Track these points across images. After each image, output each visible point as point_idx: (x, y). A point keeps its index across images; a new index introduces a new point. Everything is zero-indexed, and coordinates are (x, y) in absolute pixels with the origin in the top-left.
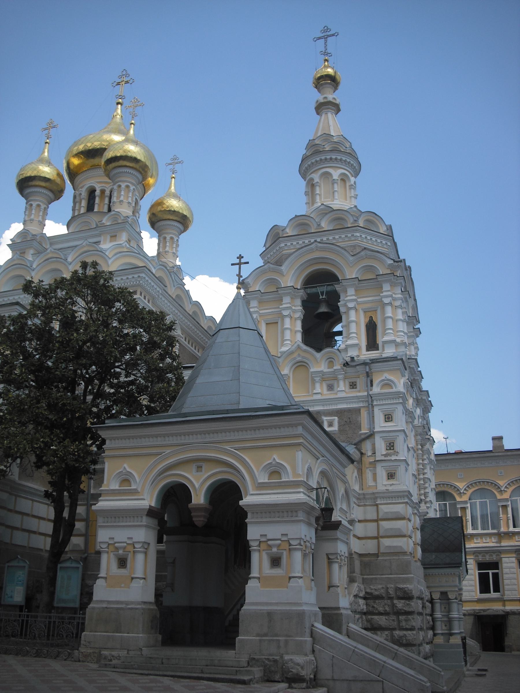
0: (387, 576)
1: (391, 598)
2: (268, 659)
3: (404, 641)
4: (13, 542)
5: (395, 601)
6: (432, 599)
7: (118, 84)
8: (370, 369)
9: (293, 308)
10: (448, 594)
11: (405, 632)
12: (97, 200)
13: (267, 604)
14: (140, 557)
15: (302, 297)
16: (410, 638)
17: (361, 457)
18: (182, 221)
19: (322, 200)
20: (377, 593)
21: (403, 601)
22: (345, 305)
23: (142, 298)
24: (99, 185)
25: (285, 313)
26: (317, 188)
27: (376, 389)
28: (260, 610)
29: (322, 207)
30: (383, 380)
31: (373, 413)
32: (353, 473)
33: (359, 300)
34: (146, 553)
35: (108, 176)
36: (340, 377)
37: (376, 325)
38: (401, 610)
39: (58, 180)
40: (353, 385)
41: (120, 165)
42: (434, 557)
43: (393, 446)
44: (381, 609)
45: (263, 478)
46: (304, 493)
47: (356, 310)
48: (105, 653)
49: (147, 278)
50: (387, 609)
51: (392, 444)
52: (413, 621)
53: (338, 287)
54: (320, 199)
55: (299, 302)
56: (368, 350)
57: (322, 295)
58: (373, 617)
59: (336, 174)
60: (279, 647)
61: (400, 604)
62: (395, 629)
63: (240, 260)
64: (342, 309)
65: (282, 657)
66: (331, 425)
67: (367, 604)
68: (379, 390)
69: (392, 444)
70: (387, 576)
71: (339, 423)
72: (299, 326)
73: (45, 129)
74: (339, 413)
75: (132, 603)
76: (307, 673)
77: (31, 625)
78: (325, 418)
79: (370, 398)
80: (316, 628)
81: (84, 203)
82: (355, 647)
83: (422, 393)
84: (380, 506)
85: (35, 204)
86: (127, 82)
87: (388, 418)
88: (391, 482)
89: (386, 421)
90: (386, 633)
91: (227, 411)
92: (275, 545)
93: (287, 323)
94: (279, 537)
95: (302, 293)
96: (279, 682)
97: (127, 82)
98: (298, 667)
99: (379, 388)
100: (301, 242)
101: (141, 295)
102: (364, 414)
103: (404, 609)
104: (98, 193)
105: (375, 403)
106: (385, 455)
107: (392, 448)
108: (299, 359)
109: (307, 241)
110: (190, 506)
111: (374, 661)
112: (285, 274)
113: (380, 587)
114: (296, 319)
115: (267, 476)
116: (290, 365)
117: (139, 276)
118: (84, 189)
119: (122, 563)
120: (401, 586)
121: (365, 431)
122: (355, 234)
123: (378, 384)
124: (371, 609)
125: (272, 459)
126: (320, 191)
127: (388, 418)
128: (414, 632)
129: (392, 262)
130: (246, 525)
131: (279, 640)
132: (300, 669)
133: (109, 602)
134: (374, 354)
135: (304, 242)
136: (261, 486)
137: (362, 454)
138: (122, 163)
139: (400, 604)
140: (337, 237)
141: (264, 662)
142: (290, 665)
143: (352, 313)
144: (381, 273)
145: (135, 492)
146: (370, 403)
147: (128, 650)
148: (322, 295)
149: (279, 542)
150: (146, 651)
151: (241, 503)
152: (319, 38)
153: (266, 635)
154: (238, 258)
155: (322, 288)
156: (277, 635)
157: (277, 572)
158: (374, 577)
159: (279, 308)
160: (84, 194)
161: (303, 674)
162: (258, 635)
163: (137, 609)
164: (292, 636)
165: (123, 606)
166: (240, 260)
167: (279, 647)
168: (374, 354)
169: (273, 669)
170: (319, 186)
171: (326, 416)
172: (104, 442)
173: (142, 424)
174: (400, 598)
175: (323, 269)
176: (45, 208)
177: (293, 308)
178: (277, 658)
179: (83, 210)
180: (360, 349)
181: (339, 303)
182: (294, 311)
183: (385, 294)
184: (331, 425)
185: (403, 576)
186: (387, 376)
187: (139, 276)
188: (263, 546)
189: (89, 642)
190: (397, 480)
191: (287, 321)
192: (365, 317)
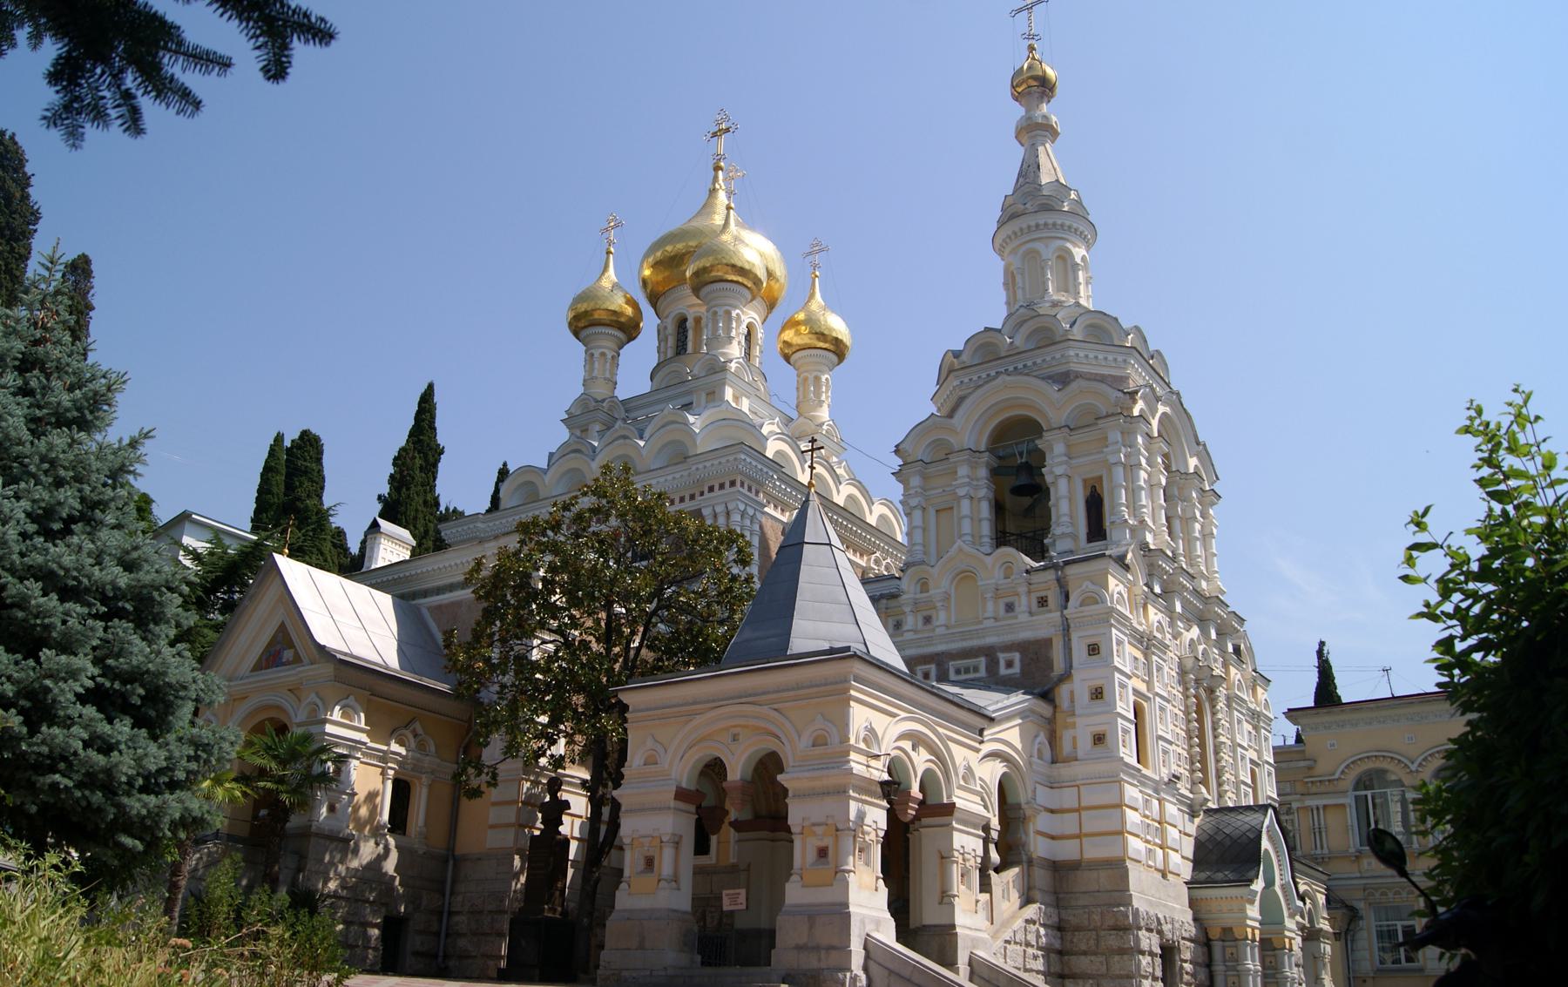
9: (975, 483)
10: (1234, 930)
12: (690, 334)
14: (668, 853)
15: (988, 464)
22: (1052, 472)
23: (745, 491)
25: (962, 492)
32: (1036, 736)
34: (677, 848)
35: (698, 297)
39: (629, 311)
43: (1101, 693)
44: (1083, 947)
49: (748, 460)
51: (1099, 690)
53: (1040, 444)
55: (983, 472)
56: (1090, 540)
57: (1021, 456)
60: (820, 960)
64: (1049, 479)
66: (1009, 664)
67: (1062, 938)
69: (1099, 690)
72: (985, 510)
74: (1023, 647)
81: (671, 341)
83: (1210, 601)
85: (597, 353)
86: (727, 130)
87: (1093, 650)
90: (1091, 981)
93: (965, 507)
95: (986, 457)
97: (727, 130)
101: (742, 485)
104: (690, 324)
109: (993, 373)
110: (724, 784)
112: (959, 430)
114: (980, 500)
117: (735, 459)
119: (649, 862)
135: (988, 375)
148: (1021, 456)
151: (780, 777)
159: (951, 485)
160: (671, 329)
167: (820, 960)
176: (613, 357)
177: (975, 483)
179: (670, 353)
180: (1074, 537)
181: (1043, 470)
182: (976, 488)
184: (1009, 664)
187: (735, 459)
191: (965, 503)
192: (1085, 487)
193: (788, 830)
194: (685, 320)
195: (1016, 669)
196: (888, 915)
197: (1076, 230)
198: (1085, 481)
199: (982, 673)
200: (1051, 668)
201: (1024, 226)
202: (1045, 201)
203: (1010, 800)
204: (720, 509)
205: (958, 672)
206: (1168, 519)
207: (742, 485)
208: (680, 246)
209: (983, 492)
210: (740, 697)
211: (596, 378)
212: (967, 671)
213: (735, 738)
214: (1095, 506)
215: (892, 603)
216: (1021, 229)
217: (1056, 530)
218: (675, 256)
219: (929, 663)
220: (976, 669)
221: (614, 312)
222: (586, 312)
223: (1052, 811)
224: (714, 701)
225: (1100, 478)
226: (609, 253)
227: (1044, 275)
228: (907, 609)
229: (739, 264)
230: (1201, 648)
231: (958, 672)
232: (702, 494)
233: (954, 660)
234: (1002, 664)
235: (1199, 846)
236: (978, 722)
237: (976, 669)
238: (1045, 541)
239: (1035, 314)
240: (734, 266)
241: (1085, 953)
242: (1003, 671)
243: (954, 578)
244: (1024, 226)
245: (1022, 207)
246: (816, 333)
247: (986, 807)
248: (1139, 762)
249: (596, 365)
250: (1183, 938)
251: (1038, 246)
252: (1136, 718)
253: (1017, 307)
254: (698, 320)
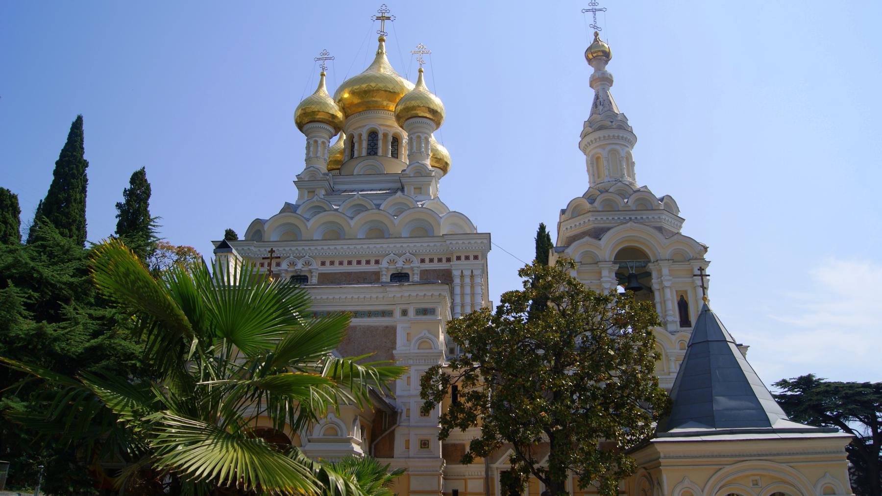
7: (378, 18)
63: (701, 272)
73: (319, 59)
86: (388, 18)
97: (388, 18)
104: (380, 136)
152: (587, 11)
154: (698, 270)
166: (701, 272)
192: (677, 296)
197: (629, 140)
198: (677, 292)
201: (611, 135)
202: (621, 124)
204: (467, 273)
208: (364, 86)
210: (767, 455)
211: (319, 157)
213: (756, 483)
216: (609, 136)
221: (333, 115)
222: (314, 112)
224: (739, 456)
225: (686, 292)
226: (323, 75)
227: (621, 165)
229: (432, 107)
240: (429, 108)
244: (611, 135)
245: (610, 124)
246: (436, 158)
249: (319, 149)
251: (618, 147)
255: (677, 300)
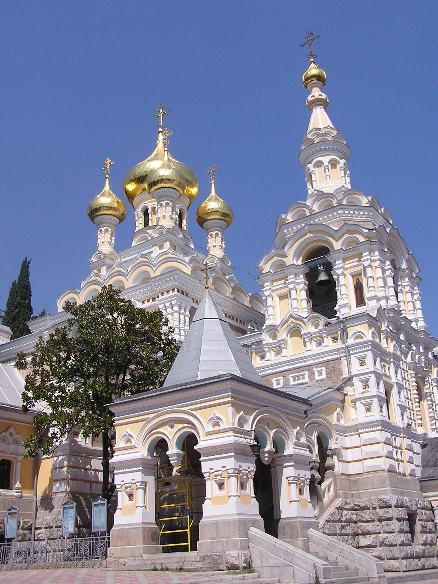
0: (370, 490)
1: (374, 508)
2: (216, 554)
3: (388, 543)
4: (92, 492)
5: (378, 510)
6: (432, 507)
8: (344, 326)
11: (387, 535)
13: (216, 516)
14: (141, 491)
16: (391, 539)
17: (345, 397)
18: (223, 218)
19: (318, 185)
20: (362, 505)
21: (383, 509)
24: (151, 204)
26: (313, 175)
27: (351, 341)
28: (211, 521)
29: (316, 192)
30: (355, 333)
31: (350, 361)
33: (346, 266)
36: (324, 335)
37: (362, 285)
38: (382, 517)
40: (335, 339)
41: (159, 187)
42: (432, 471)
43: (367, 385)
44: (368, 518)
45: (209, 428)
46: (234, 436)
47: (345, 276)
48: (121, 560)
50: (373, 517)
52: (392, 525)
54: (317, 184)
56: (357, 307)
58: (362, 524)
59: (326, 160)
60: (223, 545)
61: (381, 512)
62: (380, 533)
64: (335, 277)
65: (224, 553)
66: (320, 374)
68: (353, 341)
69: (367, 384)
70: (370, 490)
71: (326, 372)
72: (303, 295)
75: (137, 524)
76: (241, 563)
77: (79, 547)
78: (315, 369)
79: (346, 348)
80: (251, 531)
82: (276, 543)
84: (361, 435)
87: (362, 363)
88: (369, 414)
89: (361, 366)
91: (186, 384)
92: (219, 475)
94: (221, 469)
96: (224, 570)
98: (233, 559)
99: (353, 339)
100: (299, 226)
102: (344, 361)
103: (385, 516)
104: (150, 211)
105: (351, 352)
106: (362, 393)
107: (367, 387)
108: (292, 325)
110: (167, 453)
111: (287, 551)
113: (365, 499)
115: (211, 426)
116: (287, 331)
118: (139, 210)
119: (131, 496)
120: (381, 498)
121: (346, 375)
122: (339, 212)
123: (352, 337)
124: (360, 518)
125: (213, 414)
126: (316, 177)
127: (362, 363)
128: (394, 534)
129: (367, 231)
130: (200, 462)
131: (222, 541)
132: (234, 560)
133: (123, 525)
134: (362, 309)
136: (208, 434)
137: (345, 395)
138: (159, 186)
139: (381, 512)
140: (321, 219)
141: (213, 557)
142: (229, 558)
143: (341, 278)
144: (361, 242)
145: (134, 447)
146: (347, 352)
147: (135, 557)
149: (221, 472)
150: (145, 556)
151: (196, 447)
153: (215, 538)
155: (319, 260)
156: (222, 538)
157: (223, 492)
158: (361, 492)
161: (237, 564)
162: (211, 539)
163: (139, 528)
164: (231, 538)
165: (131, 527)
167: (223, 545)
168: (362, 309)
169: (219, 561)
170: (314, 174)
171: (316, 368)
172: (113, 415)
173: (133, 401)
174: (381, 507)
175: (311, 248)
178: (221, 553)
179: (141, 226)
182: (299, 284)
183: (364, 258)
184: (320, 374)
185: (383, 489)
186: (359, 328)
188: (212, 476)
189: (112, 554)
190: (372, 412)
192: (353, 280)
193: (202, 476)
194: (148, 209)
195: (324, 376)
196: (260, 517)
199: (306, 379)
200: (342, 374)
203: (324, 445)
204: (167, 304)
205: (294, 380)
206: (396, 293)
207: (178, 291)
209: (302, 286)
212: (299, 379)
214: (359, 289)
215: (259, 347)
217: (340, 302)
218: (141, 177)
219: (279, 376)
220: (303, 378)
223: (347, 449)
228: (266, 350)
230: (417, 357)
231: (294, 380)
232: (158, 297)
233: (292, 374)
234: (316, 374)
235: (423, 459)
236: (305, 407)
237: (303, 378)
238: (335, 308)
239: (322, 193)
241: (369, 521)
242: (317, 378)
243: (288, 334)
247: (311, 452)
248: (389, 419)
250: (420, 508)
252: (386, 397)
253: (313, 190)
254: (154, 209)
255: (353, 283)
